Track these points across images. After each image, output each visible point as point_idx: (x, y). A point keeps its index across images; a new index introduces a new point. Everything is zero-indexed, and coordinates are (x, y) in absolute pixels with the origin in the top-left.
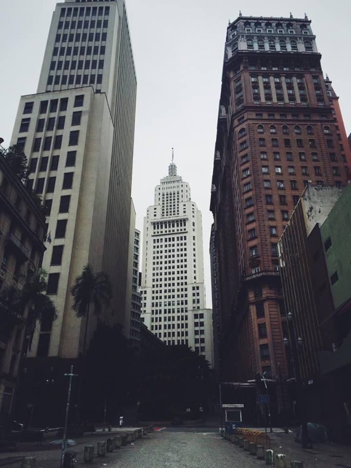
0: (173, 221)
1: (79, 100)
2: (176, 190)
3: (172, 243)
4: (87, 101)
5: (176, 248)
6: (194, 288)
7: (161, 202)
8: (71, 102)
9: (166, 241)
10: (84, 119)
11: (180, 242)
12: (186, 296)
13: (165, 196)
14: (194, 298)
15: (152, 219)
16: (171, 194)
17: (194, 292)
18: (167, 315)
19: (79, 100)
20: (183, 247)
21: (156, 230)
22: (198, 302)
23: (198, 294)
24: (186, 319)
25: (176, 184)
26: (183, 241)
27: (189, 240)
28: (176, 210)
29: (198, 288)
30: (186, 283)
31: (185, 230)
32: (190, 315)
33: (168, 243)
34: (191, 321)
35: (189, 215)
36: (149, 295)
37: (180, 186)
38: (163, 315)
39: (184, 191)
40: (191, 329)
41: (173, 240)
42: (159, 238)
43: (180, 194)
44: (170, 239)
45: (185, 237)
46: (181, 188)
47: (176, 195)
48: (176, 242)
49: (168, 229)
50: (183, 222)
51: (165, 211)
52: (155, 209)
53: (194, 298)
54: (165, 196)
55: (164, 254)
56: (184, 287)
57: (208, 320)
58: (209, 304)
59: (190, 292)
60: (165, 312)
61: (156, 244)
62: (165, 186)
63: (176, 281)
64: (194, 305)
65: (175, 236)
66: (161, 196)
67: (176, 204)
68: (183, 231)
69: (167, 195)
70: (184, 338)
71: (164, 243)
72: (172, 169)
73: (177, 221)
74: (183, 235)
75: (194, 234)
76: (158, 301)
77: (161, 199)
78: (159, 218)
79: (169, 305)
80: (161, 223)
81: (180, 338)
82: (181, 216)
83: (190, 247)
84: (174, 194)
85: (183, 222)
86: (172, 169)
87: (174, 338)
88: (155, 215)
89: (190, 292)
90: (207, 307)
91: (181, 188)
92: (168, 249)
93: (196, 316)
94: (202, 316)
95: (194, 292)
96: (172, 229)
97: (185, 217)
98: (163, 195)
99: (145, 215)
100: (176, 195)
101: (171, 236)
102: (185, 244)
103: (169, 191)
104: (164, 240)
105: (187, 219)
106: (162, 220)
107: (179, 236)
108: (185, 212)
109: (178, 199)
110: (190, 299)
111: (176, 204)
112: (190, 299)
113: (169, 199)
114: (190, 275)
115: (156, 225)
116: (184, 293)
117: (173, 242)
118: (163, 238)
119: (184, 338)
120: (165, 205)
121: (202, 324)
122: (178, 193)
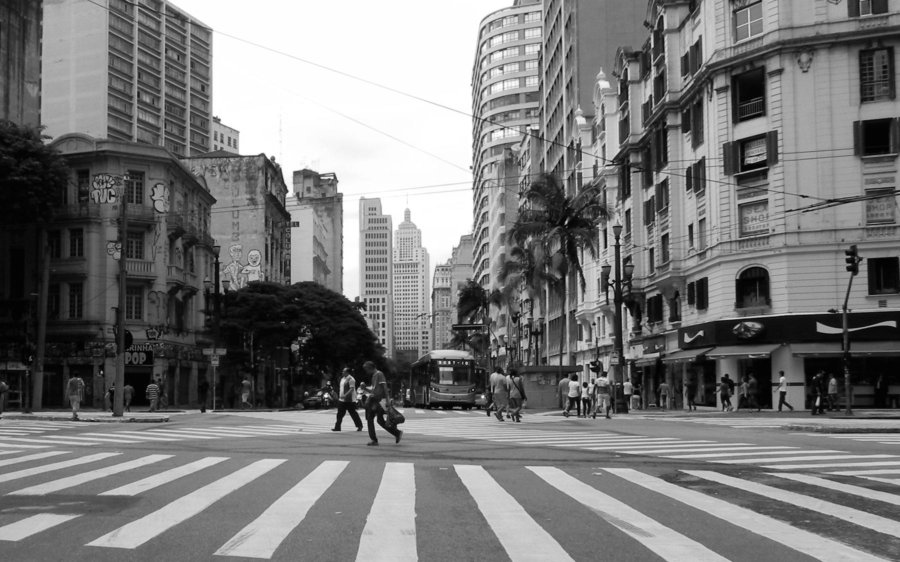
1: (384, 299)
4: (386, 300)
8: (381, 300)
10: (386, 308)
19: (384, 299)
27: (420, 279)
32: (420, 333)
34: (420, 336)
40: (420, 340)
55: (402, 288)
71: (402, 280)
72: (408, 213)
75: (424, 274)
82: (414, 261)
83: (420, 284)
85: (416, 265)
86: (408, 213)
93: (423, 333)
115: (397, 266)
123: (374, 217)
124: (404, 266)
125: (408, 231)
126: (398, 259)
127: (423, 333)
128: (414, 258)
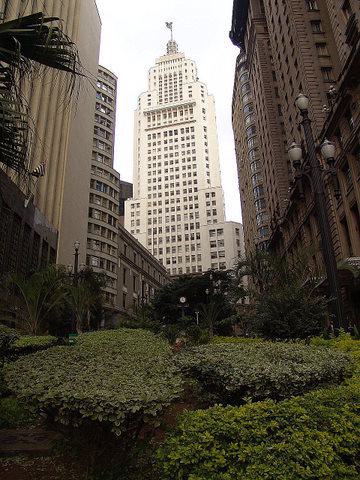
0: (175, 108)
2: (177, 71)
3: (174, 137)
5: (180, 143)
7: (158, 88)
9: (166, 135)
11: (185, 135)
13: (163, 80)
14: (209, 208)
15: (145, 107)
16: (170, 76)
18: (170, 234)
20: (191, 141)
21: (152, 123)
22: (215, 214)
23: (214, 203)
24: (198, 238)
25: (177, 64)
26: (190, 134)
27: (199, 133)
28: (178, 91)
29: (213, 194)
30: (196, 190)
33: (169, 138)
35: (197, 98)
36: (143, 209)
38: (164, 235)
39: (189, 71)
41: (176, 134)
42: (155, 132)
44: (171, 132)
46: (184, 68)
47: (178, 76)
48: (179, 136)
49: (168, 119)
50: (190, 106)
51: (163, 98)
53: (209, 208)
54: (163, 80)
56: (193, 194)
57: (228, 237)
58: (233, 211)
59: (202, 201)
60: (168, 230)
61: (152, 141)
62: (163, 67)
63: (181, 188)
64: (210, 218)
65: (178, 128)
66: (157, 80)
67: (178, 87)
68: (190, 120)
70: (196, 264)
71: (162, 139)
72: (172, 47)
73: (180, 107)
74: (190, 125)
76: (157, 215)
77: (158, 83)
78: (155, 106)
79: (173, 219)
80: (158, 112)
81: (190, 264)
82: (186, 99)
83: (199, 141)
85: (190, 106)
86: (172, 47)
87: (181, 265)
89: (202, 201)
90: (228, 219)
91: (184, 68)
94: (220, 231)
96: (173, 119)
98: (160, 78)
99: (136, 106)
100: (178, 76)
101: (173, 129)
102: (193, 137)
103: (168, 73)
104: (162, 134)
107: (184, 126)
111: (178, 87)
113: (168, 82)
114: (202, 177)
116: (193, 202)
117: (176, 137)
118: (162, 131)
119: (196, 264)
120: (164, 90)
121: (222, 243)
124: (167, 112)
125: (172, 64)
128: (185, 95)
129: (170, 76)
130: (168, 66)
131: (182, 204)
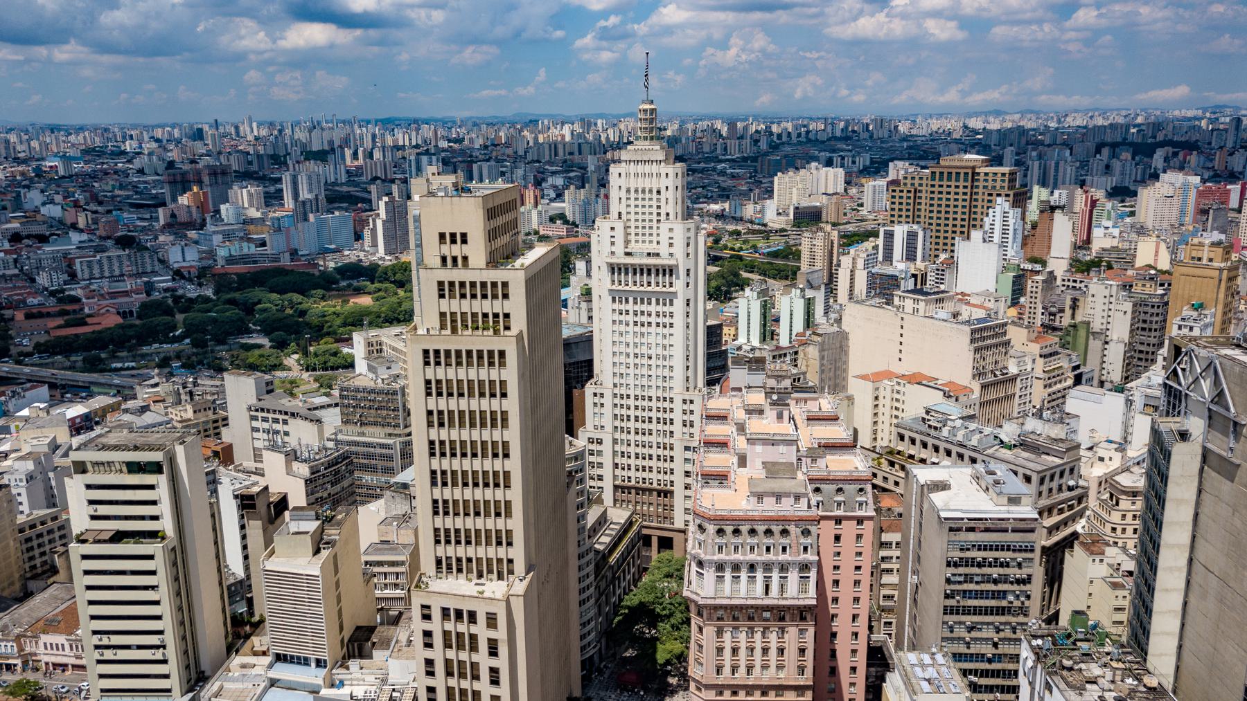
6: (685, 402)
12: (672, 410)
13: (633, 195)
14: (685, 418)
16: (643, 191)
17: (685, 407)
20: (667, 320)
24: (672, 449)
31: (671, 285)
37: (663, 175)
43: (663, 197)
45: (671, 301)
46: (664, 182)
47: (655, 196)
52: (612, 229)
53: (685, 418)
54: (633, 195)
66: (623, 194)
69: (636, 191)
70: (667, 477)
81: (660, 477)
84: (651, 191)
88: (613, 243)
89: (678, 406)
92: (639, 319)
95: (685, 407)
97: (672, 262)
98: (628, 191)
105: (677, 266)
106: (629, 260)
108: (671, 245)
109: (659, 207)
110: (678, 416)
112: (678, 416)
122: (659, 192)
123: (457, 275)
125: (647, 168)
126: (619, 249)
127: (687, 448)
129: (643, 191)
130: (640, 168)
131: (654, 404)
